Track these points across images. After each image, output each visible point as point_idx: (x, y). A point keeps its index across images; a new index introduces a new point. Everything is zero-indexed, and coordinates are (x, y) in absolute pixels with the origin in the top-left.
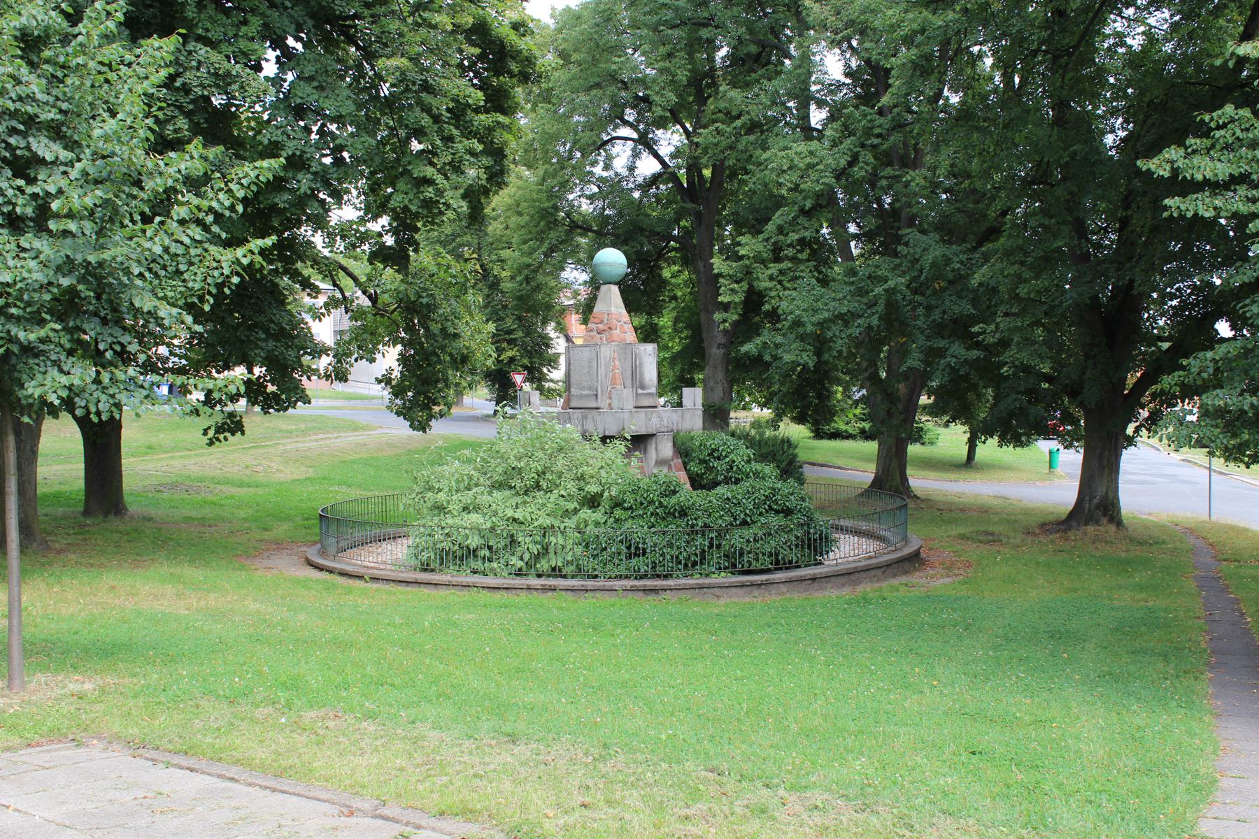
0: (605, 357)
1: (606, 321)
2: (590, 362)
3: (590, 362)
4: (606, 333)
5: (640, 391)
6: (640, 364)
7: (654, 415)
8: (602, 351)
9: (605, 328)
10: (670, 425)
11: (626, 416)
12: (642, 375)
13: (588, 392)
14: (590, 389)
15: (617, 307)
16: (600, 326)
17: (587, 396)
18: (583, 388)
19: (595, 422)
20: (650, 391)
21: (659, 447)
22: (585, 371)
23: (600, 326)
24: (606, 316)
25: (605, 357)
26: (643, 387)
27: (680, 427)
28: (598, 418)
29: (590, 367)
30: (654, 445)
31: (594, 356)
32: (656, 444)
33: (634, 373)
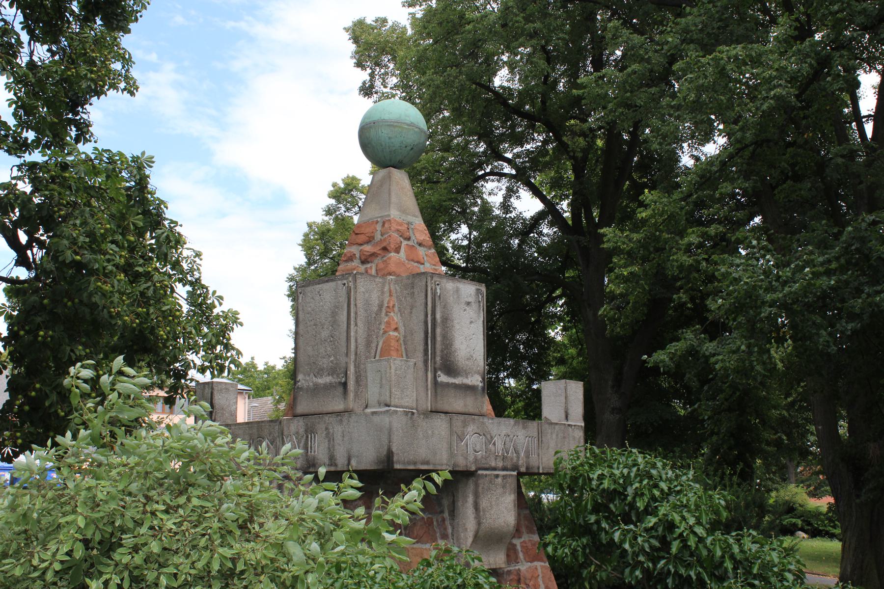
0: (367, 303)
1: (378, 237)
2: (334, 314)
3: (334, 314)
4: (378, 260)
5: (443, 378)
6: (446, 319)
7: (471, 428)
8: (361, 289)
9: (376, 250)
10: (511, 454)
11: (398, 423)
12: (448, 344)
13: (326, 380)
14: (333, 371)
15: (404, 211)
16: (368, 248)
17: (328, 387)
18: (319, 372)
19: (330, 437)
20: (469, 381)
21: (484, 503)
22: (325, 334)
23: (368, 248)
24: (379, 227)
25: (367, 303)
26: (450, 369)
27: (534, 461)
28: (337, 430)
29: (334, 323)
30: (471, 499)
31: (343, 299)
32: (477, 496)
33: (429, 336)
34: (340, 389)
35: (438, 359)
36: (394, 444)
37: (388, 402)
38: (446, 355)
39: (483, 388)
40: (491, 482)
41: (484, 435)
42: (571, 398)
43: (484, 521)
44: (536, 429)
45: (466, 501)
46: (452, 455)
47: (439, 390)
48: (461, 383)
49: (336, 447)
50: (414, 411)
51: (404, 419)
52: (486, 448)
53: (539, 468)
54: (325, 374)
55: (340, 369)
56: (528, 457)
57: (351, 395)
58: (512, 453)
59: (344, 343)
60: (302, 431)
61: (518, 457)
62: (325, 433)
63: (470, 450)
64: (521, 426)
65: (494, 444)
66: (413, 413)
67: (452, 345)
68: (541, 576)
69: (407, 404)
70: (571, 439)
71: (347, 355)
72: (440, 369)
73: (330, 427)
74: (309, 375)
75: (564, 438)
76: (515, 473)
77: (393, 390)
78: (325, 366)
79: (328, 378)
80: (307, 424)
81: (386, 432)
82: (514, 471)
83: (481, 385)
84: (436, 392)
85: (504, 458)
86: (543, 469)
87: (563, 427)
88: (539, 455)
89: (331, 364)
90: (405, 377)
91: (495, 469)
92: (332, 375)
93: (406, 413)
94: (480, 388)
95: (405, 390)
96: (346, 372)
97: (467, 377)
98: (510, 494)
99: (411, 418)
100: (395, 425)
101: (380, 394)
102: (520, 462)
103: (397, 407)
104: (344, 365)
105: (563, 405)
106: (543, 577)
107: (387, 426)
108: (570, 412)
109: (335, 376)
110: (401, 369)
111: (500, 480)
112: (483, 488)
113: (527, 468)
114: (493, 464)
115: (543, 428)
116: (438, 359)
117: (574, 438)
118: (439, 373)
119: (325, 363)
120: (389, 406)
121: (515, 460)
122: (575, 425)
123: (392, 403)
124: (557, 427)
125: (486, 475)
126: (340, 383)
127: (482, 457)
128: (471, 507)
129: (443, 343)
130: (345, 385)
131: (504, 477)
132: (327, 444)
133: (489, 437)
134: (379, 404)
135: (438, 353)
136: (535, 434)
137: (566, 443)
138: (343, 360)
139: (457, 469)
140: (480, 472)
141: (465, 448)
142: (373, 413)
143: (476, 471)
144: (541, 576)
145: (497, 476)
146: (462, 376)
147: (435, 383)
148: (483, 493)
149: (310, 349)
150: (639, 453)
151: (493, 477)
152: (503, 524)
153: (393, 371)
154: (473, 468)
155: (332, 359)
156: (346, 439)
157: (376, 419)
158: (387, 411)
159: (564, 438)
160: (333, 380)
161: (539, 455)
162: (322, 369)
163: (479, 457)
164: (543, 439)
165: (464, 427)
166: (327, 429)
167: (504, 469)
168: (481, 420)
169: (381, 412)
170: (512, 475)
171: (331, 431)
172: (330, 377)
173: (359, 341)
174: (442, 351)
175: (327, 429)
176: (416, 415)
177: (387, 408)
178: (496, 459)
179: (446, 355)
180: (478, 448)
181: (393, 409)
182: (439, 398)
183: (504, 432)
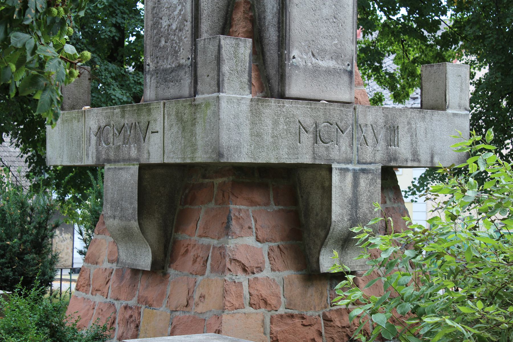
13: (331, 64)
17: (329, 72)
19: (413, 134)
49: (419, 143)
54: (328, 57)
55: (345, 56)
62: (407, 127)
73: (413, 123)
78: (327, 48)
101: (461, 98)
109: (340, 62)
126: (345, 71)
132: (409, 139)
142: (455, 115)
149: (308, 23)
150: (129, 165)
155: (336, 42)
156: (429, 136)
160: (337, 66)
162: (325, 51)
166: (409, 123)
172: (334, 62)
175: (409, 123)
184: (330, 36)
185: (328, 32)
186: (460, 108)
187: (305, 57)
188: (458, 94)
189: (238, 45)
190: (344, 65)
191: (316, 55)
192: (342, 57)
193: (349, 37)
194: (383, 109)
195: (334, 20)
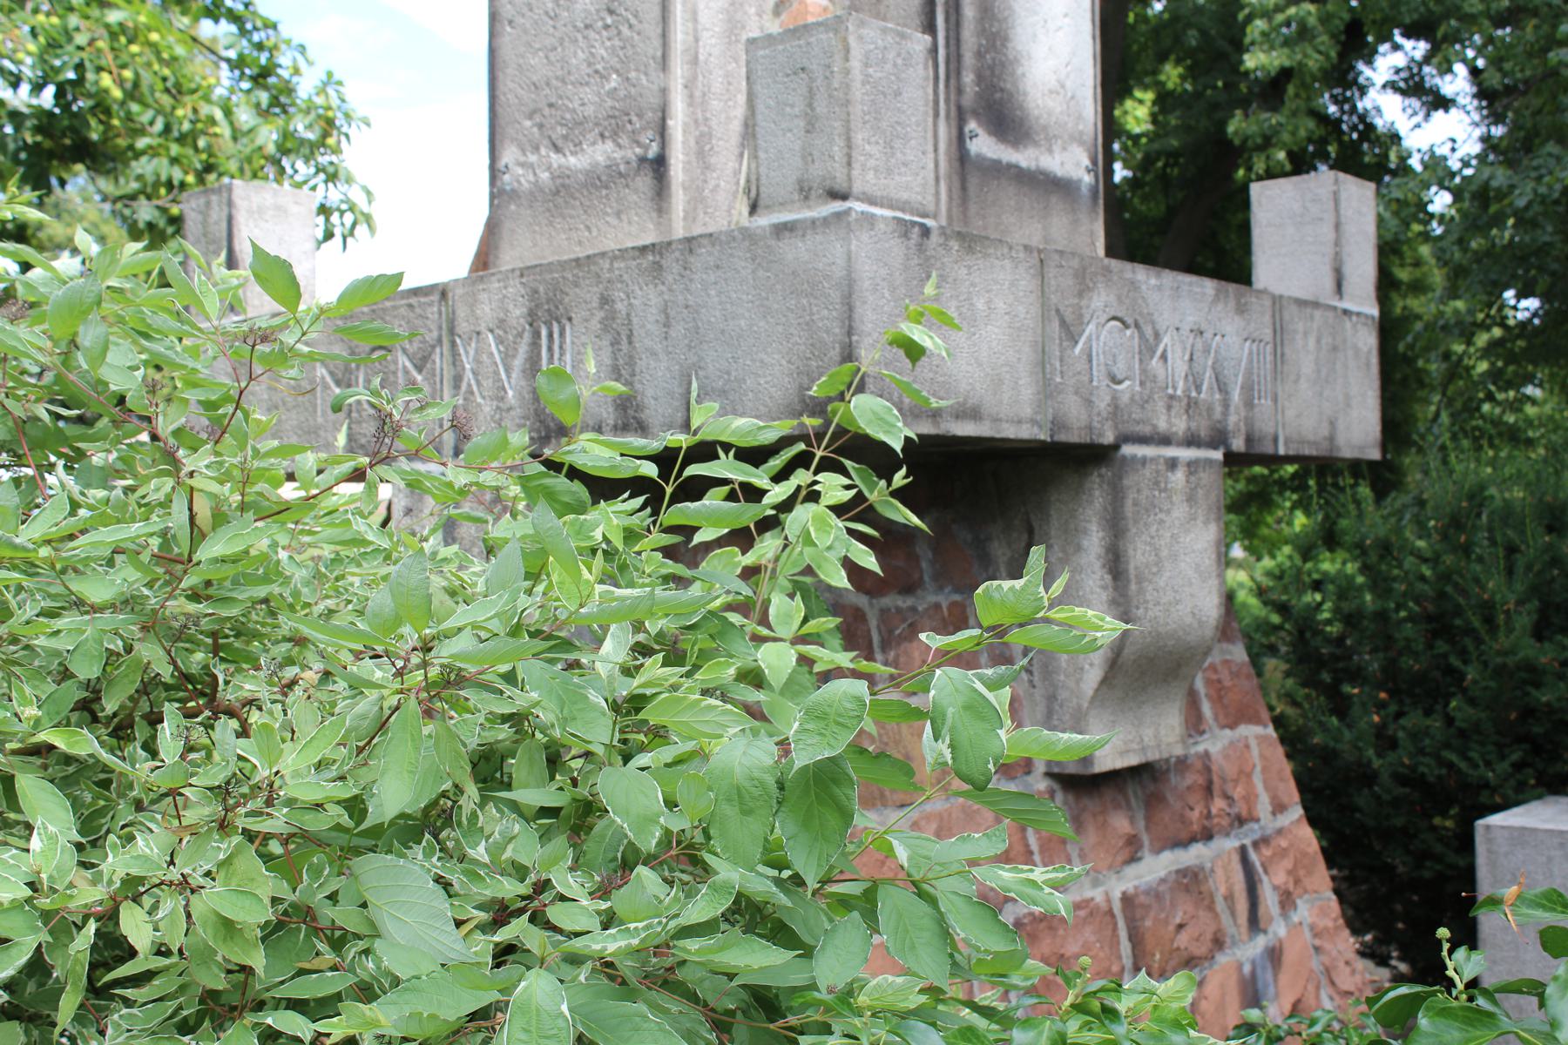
5: (983, 145)
13: (599, 153)
14: (613, 127)
17: (601, 181)
21: (1138, 555)
27: (1265, 422)
30: (1094, 541)
32: (1116, 528)
34: (644, 182)
35: (968, 78)
36: (868, 341)
37: (840, 183)
38: (992, 68)
39: (1094, 191)
40: (1157, 483)
41: (1137, 326)
42: (1350, 229)
43: (1140, 612)
44: (1267, 319)
45: (1079, 548)
46: (1047, 390)
47: (973, 181)
48: (1033, 166)
49: (641, 365)
50: (929, 222)
51: (896, 249)
52: (1144, 371)
53: (1276, 440)
55: (640, 116)
56: (1249, 404)
57: (679, 199)
58: (1211, 388)
59: (653, 31)
60: (517, 312)
61: (1226, 404)
62: (600, 315)
63: (1099, 374)
64: (1232, 304)
65: (1164, 357)
66: (926, 232)
67: (1006, 39)
68: (1258, 769)
69: (905, 196)
70: (1350, 353)
71: (664, 63)
72: (976, 114)
74: (536, 149)
75: (1335, 349)
76: (1218, 455)
77: (858, 137)
78: (589, 111)
79: (600, 146)
80: (536, 292)
81: (836, 296)
82: (1215, 448)
83: (1088, 179)
84: (964, 188)
85: (1191, 405)
86: (1286, 443)
87: (1330, 314)
88: (1275, 400)
89: (610, 103)
90: (898, 94)
91: (1165, 441)
92: (615, 136)
93: (904, 228)
94: (1085, 190)
95: (897, 144)
96: (664, 119)
97: (1050, 151)
98: (1206, 523)
99: (921, 248)
100: (866, 269)
101: (807, 156)
102: (1232, 419)
103: (872, 201)
104: (655, 101)
105: (1329, 250)
106: (1264, 770)
107: (838, 272)
108: (1347, 270)
109: (624, 140)
110: (884, 60)
111: (1179, 477)
112: (1136, 504)
113: (1249, 440)
114: (1162, 425)
115: (1286, 316)
116: (968, 78)
117: (1357, 351)
118: (972, 125)
119: (588, 100)
120: (844, 197)
121: (1217, 414)
122: (1358, 314)
123: (857, 187)
124: (1318, 313)
125: (1144, 461)
126: (642, 160)
127: (1132, 399)
128: (1097, 565)
129: (982, 31)
130: (659, 165)
131: (1192, 466)
133: (1148, 331)
134: (805, 193)
135: (969, 59)
136: (1267, 333)
137: (1339, 366)
138: (648, 84)
139: (1062, 437)
140: (1128, 450)
141: (1081, 366)
142: (782, 229)
143: (1115, 447)
144: (1258, 769)
145: (1172, 464)
146: (1036, 144)
147: (962, 158)
148: (1136, 522)
151: (1162, 467)
152: (1188, 620)
153: (855, 64)
154: (1109, 438)
155: (613, 84)
156: (678, 330)
157: (795, 250)
158: (839, 216)
159: (1335, 349)
160: (618, 155)
161: (1275, 400)
163: (1125, 399)
164: (1287, 351)
165: (1080, 295)
166: (605, 301)
167: (1191, 441)
168: (1128, 275)
169: (813, 222)
170: (1209, 462)
171: (619, 306)
172: (609, 146)
173: (705, 17)
174: (979, 55)
175: (605, 301)
176: (935, 238)
177: (837, 206)
178: (1169, 408)
179: (992, 68)
180: (1120, 369)
181: (859, 206)
182: (973, 209)
183: (1190, 320)
184: (597, 72)
185: (590, 64)
186: (807, 198)
187: (533, 158)
188: (797, 146)
189: (208, 204)
190: (639, 144)
191: (560, 143)
192: (630, 122)
193: (651, 52)
194: (522, 275)
195: (609, 21)
